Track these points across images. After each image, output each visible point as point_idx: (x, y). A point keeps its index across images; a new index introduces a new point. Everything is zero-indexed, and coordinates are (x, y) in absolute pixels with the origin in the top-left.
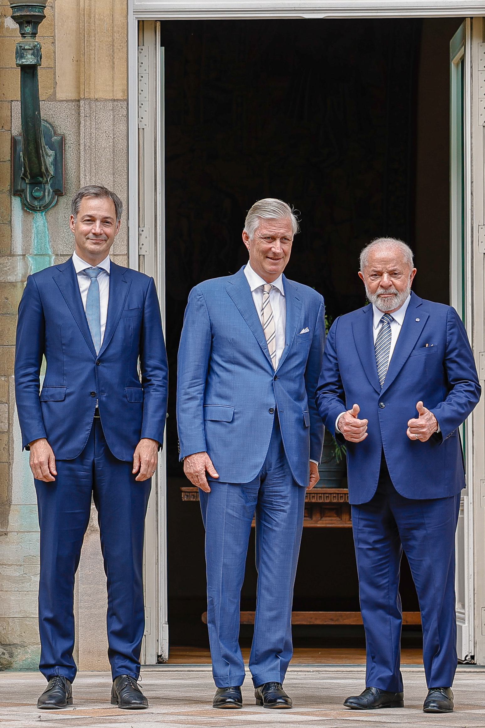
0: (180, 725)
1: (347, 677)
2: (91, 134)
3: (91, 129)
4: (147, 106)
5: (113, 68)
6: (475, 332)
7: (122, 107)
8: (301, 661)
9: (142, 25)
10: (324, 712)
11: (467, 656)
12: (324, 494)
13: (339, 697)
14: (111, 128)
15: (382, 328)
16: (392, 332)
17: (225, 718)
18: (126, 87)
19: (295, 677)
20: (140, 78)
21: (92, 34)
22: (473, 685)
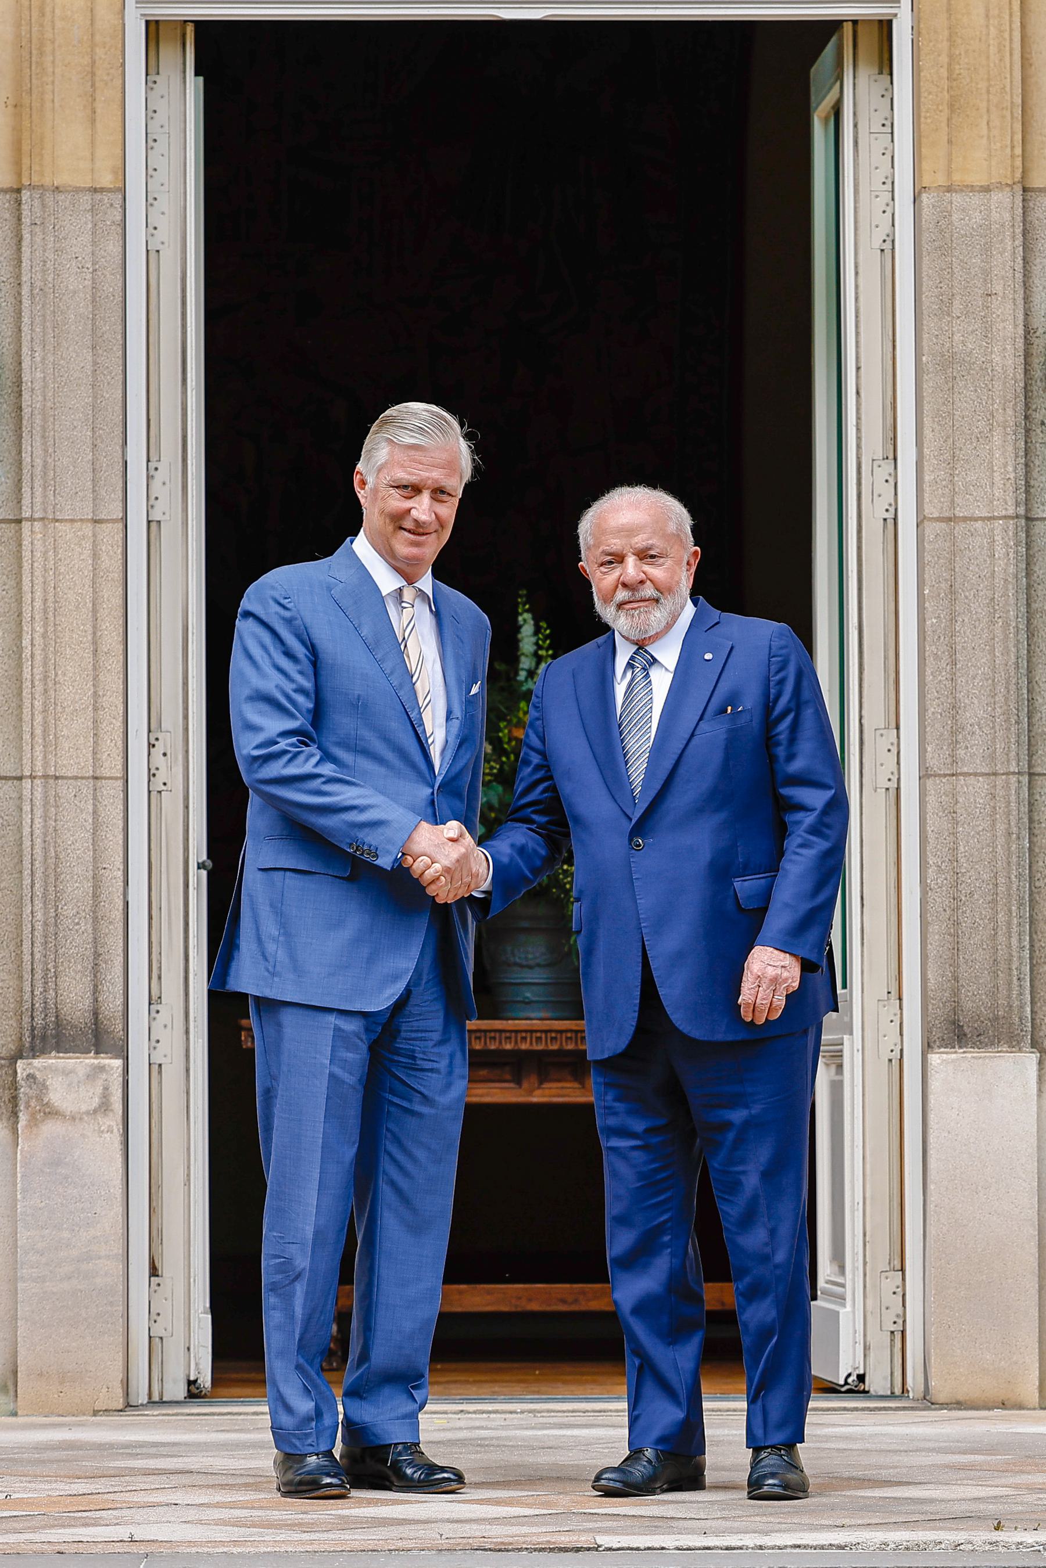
0: (236, 1529)
1: (595, 1422)
2: (45, 262)
3: (44, 251)
4: (163, 203)
5: (93, 121)
6: (865, 685)
7: (112, 205)
8: (496, 1389)
9: (154, 29)
10: (543, 1498)
11: (849, 1375)
12: (546, 1032)
13: (577, 1466)
14: (89, 249)
15: (632, 680)
16: (654, 686)
17: (333, 1512)
18: (119, 163)
19: (483, 1424)
20: (151, 143)
21: (48, 49)
22: (862, 1438)
